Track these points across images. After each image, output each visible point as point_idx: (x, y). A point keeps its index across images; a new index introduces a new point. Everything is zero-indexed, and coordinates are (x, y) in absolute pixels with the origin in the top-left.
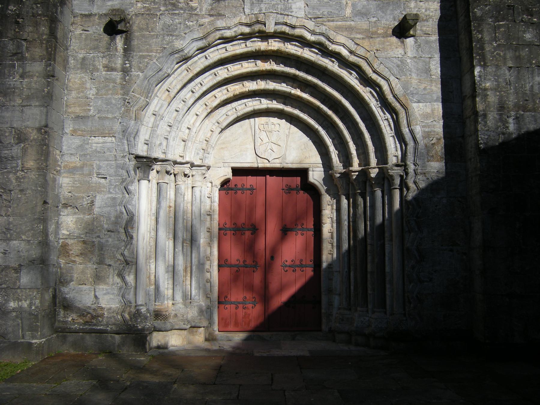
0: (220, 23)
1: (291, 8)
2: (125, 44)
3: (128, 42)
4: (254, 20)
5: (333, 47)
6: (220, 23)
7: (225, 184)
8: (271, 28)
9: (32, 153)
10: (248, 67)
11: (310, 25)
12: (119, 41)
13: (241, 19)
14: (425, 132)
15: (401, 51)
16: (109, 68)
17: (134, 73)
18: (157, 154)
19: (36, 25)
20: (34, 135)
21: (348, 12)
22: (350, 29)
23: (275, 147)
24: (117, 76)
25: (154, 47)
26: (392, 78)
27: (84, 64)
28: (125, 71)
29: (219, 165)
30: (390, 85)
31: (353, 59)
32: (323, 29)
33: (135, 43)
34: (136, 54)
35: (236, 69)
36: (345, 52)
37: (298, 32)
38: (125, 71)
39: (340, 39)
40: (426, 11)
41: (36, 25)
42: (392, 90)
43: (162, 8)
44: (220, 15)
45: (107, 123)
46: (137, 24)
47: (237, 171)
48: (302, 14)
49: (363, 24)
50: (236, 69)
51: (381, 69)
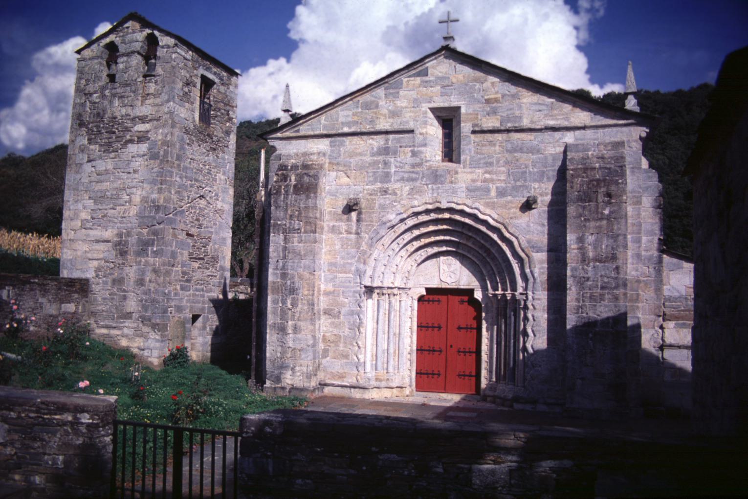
1: (457, 192)
2: (357, 217)
3: (360, 214)
4: (435, 200)
7: (421, 299)
8: (444, 205)
10: (432, 228)
11: (468, 202)
12: (354, 215)
13: (426, 200)
14: (540, 272)
16: (349, 232)
17: (363, 234)
18: (376, 284)
23: (452, 275)
24: (353, 236)
25: (374, 219)
26: (520, 237)
27: (333, 230)
29: (417, 286)
30: (519, 242)
32: (477, 205)
33: (363, 216)
35: (424, 230)
38: (357, 233)
40: (546, 189)
42: (520, 244)
43: (379, 194)
46: (363, 204)
47: (428, 290)
50: (424, 230)
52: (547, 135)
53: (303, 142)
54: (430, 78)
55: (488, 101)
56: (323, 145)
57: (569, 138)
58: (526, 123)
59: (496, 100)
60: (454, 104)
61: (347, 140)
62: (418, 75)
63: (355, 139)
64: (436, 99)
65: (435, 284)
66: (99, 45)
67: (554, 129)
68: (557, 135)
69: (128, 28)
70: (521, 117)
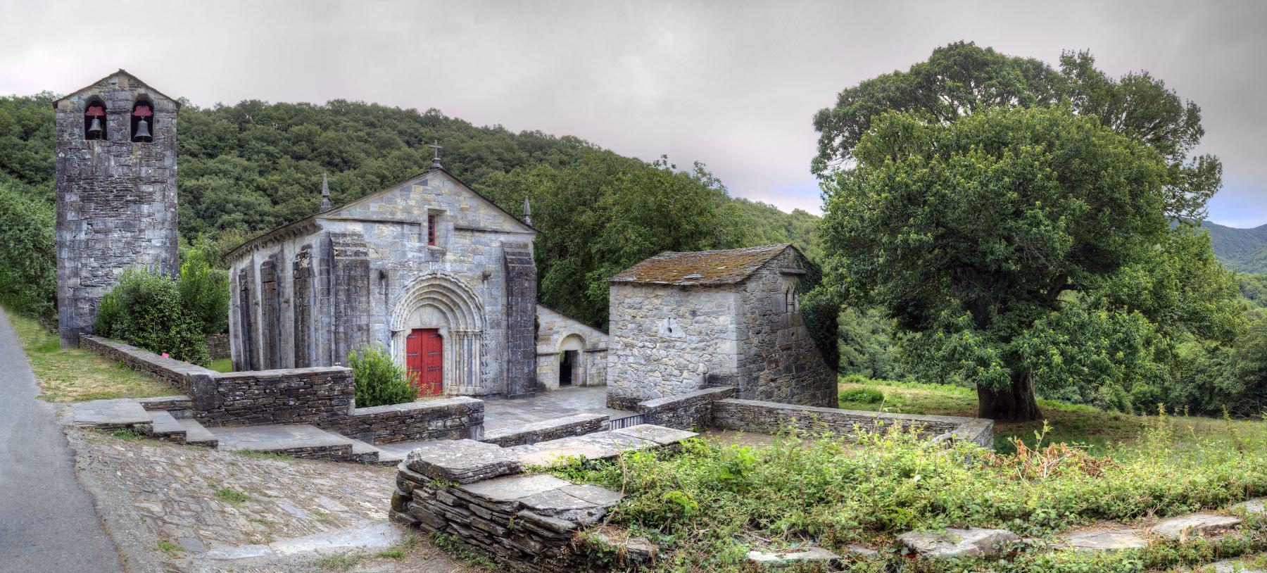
0: (421, 274)
5: (460, 284)
6: (421, 274)
8: (439, 276)
9: (365, 334)
11: (452, 275)
15: (482, 286)
16: (380, 294)
17: (390, 296)
19: (363, 280)
20: (365, 327)
21: (465, 269)
22: (466, 276)
24: (383, 297)
28: (386, 295)
31: (466, 289)
34: (390, 288)
36: (464, 286)
37: (448, 277)
39: (462, 280)
41: (363, 280)
44: (421, 271)
45: (381, 318)
46: (391, 273)
47: (414, 331)
48: (449, 270)
49: (470, 274)
51: (476, 293)
52: (492, 236)
53: (343, 224)
54: (429, 188)
55: (462, 209)
56: (358, 228)
57: (503, 238)
58: (482, 225)
59: (467, 209)
60: (443, 208)
61: (377, 225)
62: (420, 184)
63: (381, 226)
64: (432, 203)
65: (418, 325)
66: (79, 98)
67: (496, 232)
68: (497, 236)
69: (113, 84)
70: (479, 222)
